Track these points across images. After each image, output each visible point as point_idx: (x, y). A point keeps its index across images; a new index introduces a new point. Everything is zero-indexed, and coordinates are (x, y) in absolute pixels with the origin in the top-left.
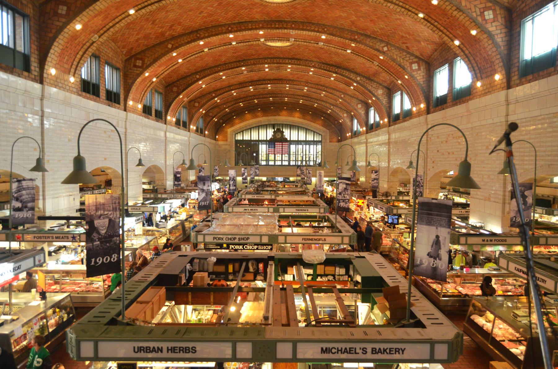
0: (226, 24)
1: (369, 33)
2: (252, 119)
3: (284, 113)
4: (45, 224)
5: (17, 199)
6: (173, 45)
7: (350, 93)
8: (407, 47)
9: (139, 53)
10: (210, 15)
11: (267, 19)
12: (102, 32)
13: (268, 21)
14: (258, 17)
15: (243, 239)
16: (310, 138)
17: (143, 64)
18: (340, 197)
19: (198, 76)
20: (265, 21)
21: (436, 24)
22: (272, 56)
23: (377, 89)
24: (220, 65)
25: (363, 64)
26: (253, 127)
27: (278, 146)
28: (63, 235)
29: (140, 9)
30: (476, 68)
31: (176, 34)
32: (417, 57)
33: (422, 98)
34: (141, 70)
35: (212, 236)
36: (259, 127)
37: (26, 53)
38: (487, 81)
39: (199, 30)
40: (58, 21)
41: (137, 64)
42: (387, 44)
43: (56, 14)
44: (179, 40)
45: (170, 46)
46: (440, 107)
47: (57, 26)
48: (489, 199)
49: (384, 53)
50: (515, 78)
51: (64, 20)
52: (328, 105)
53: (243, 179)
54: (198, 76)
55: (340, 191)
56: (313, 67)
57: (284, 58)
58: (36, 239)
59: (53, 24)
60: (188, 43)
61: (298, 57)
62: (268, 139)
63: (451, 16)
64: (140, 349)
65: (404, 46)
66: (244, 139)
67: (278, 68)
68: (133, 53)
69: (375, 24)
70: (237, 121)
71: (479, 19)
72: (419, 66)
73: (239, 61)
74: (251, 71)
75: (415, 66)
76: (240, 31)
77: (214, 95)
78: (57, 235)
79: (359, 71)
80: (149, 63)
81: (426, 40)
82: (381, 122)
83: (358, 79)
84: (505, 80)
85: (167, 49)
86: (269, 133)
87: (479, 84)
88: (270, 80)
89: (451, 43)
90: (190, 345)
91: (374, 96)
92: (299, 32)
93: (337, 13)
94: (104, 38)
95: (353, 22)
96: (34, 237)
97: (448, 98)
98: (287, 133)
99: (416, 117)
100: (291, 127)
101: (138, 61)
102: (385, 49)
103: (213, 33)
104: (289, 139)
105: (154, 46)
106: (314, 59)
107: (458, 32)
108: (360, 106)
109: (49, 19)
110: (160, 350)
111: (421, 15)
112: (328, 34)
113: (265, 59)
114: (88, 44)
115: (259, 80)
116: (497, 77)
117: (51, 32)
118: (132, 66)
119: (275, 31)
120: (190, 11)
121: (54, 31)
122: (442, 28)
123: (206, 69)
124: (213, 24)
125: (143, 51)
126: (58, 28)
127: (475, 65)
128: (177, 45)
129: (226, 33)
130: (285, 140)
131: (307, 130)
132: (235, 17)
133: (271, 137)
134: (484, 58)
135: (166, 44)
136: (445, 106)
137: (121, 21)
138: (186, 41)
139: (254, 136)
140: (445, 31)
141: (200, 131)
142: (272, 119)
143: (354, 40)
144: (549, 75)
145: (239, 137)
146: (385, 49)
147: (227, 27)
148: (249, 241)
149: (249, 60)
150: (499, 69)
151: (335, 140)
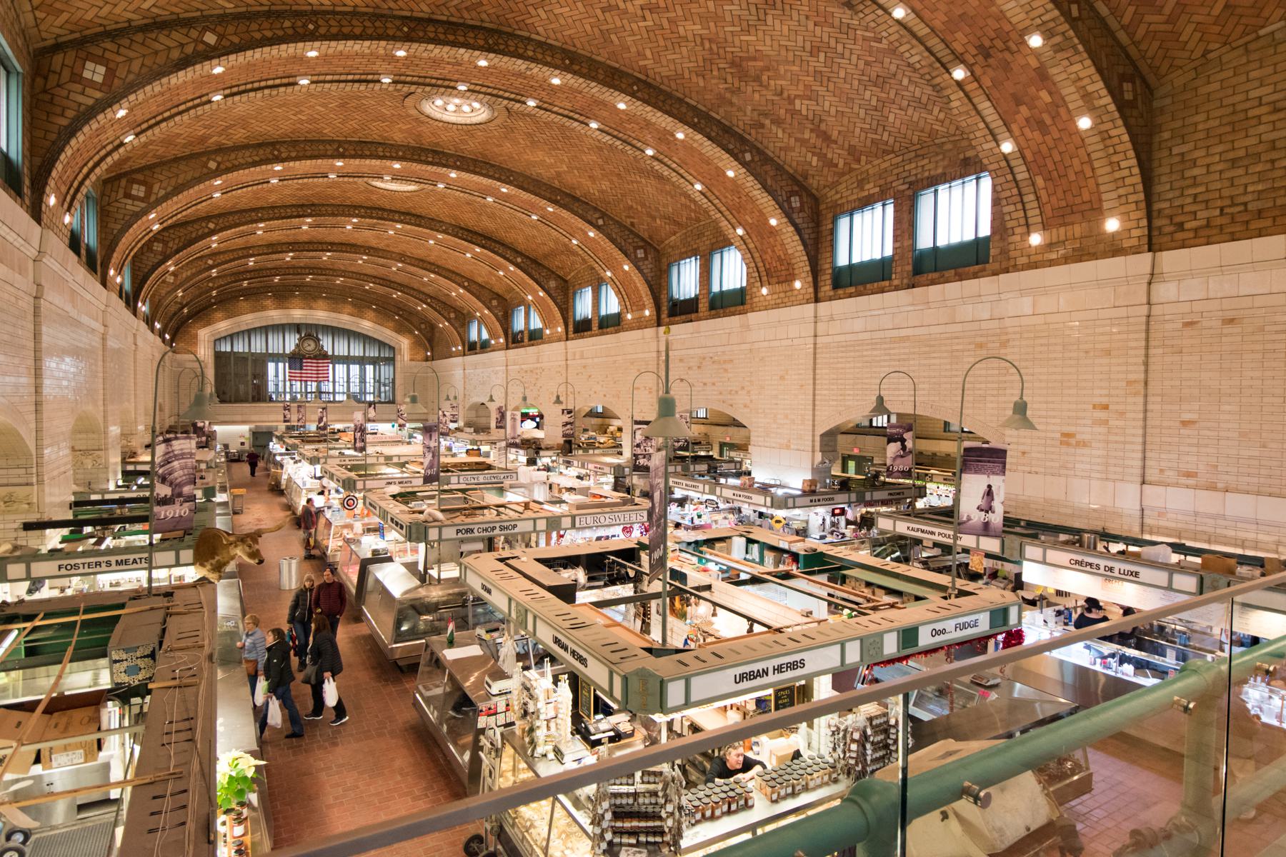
0: (333, 141)
1: (578, 193)
2: (253, 312)
3: (321, 303)
4: (43, 536)
5: (163, 480)
6: (219, 164)
7: (480, 280)
8: (632, 224)
9: (140, 170)
10: (312, 120)
11: (413, 144)
12: (145, 126)
13: (414, 148)
14: (398, 137)
15: (486, 530)
16: (373, 352)
17: (149, 192)
18: (638, 451)
19: (211, 226)
20: (408, 147)
21: (716, 201)
22: (369, 204)
23: (548, 279)
24: (262, 208)
25: (534, 237)
26: (255, 329)
27: (309, 366)
28: (137, 556)
29: (233, 95)
30: (762, 269)
31: (230, 144)
32: (643, 240)
33: (648, 300)
34: (143, 205)
35: (454, 529)
36: (266, 330)
37: (13, 155)
38: (778, 288)
39: (278, 142)
40: (83, 93)
41: (134, 192)
42: (604, 215)
43: (77, 78)
44: (233, 156)
45: (213, 165)
46: (683, 317)
47: (80, 104)
48: (788, 447)
49: (597, 227)
50: (826, 288)
51: (98, 95)
52: (422, 297)
53: (318, 428)
54: (211, 226)
55: (638, 441)
56: (445, 232)
57: (391, 211)
58: (63, 572)
59: (68, 98)
60: (255, 164)
61: (418, 211)
62: (287, 351)
63: (747, 195)
64: (743, 677)
65: (629, 221)
66: (235, 350)
67: (372, 228)
68: (126, 168)
69: (594, 183)
70: (219, 315)
71: (786, 205)
72: (646, 253)
73: (302, 206)
74: (318, 226)
75: (640, 253)
76: (362, 157)
77: (210, 262)
78: (119, 558)
79: (521, 248)
80: (162, 192)
81: (666, 218)
82: (548, 332)
83: (519, 260)
84: (811, 290)
85: (205, 170)
86: (290, 343)
87: (764, 291)
88: (332, 244)
89: (731, 231)
90: (797, 657)
91: (543, 289)
92: (465, 175)
93: (539, 156)
94: (143, 138)
95: (559, 174)
96: (60, 567)
97: (700, 306)
98: (327, 343)
99: (632, 329)
100: (335, 331)
101: (135, 186)
102: (600, 222)
103: (308, 154)
104: (330, 353)
105: (176, 160)
106: (448, 220)
107: (747, 217)
108: (495, 303)
109: (58, 86)
110: (766, 672)
111: (698, 187)
112: (516, 186)
113: (355, 207)
114: (110, 147)
115: (310, 243)
116: (798, 285)
117: (63, 115)
118: (121, 192)
119: (424, 167)
120: (280, 106)
121: (70, 114)
122: (723, 209)
123: (230, 213)
124: (310, 136)
125: (151, 167)
126: (83, 108)
127: (760, 264)
128: (229, 165)
129: (333, 157)
130: (325, 356)
131: (366, 339)
132: (355, 131)
133: (293, 347)
134: (779, 257)
135: (204, 159)
136: (693, 316)
137: (187, 110)
138: (250, 160)
139: (258, 345)
140: (727, 213)
141: (161, 335)
142: (298, 314)
143: (554, 202)
144: (882, 291)
145: (225, 347)
146: (600, 222)
147: (335, 146)
148: (516, 530)
149: (323, 205)
150: (803, 275)
151: (420, 356)
